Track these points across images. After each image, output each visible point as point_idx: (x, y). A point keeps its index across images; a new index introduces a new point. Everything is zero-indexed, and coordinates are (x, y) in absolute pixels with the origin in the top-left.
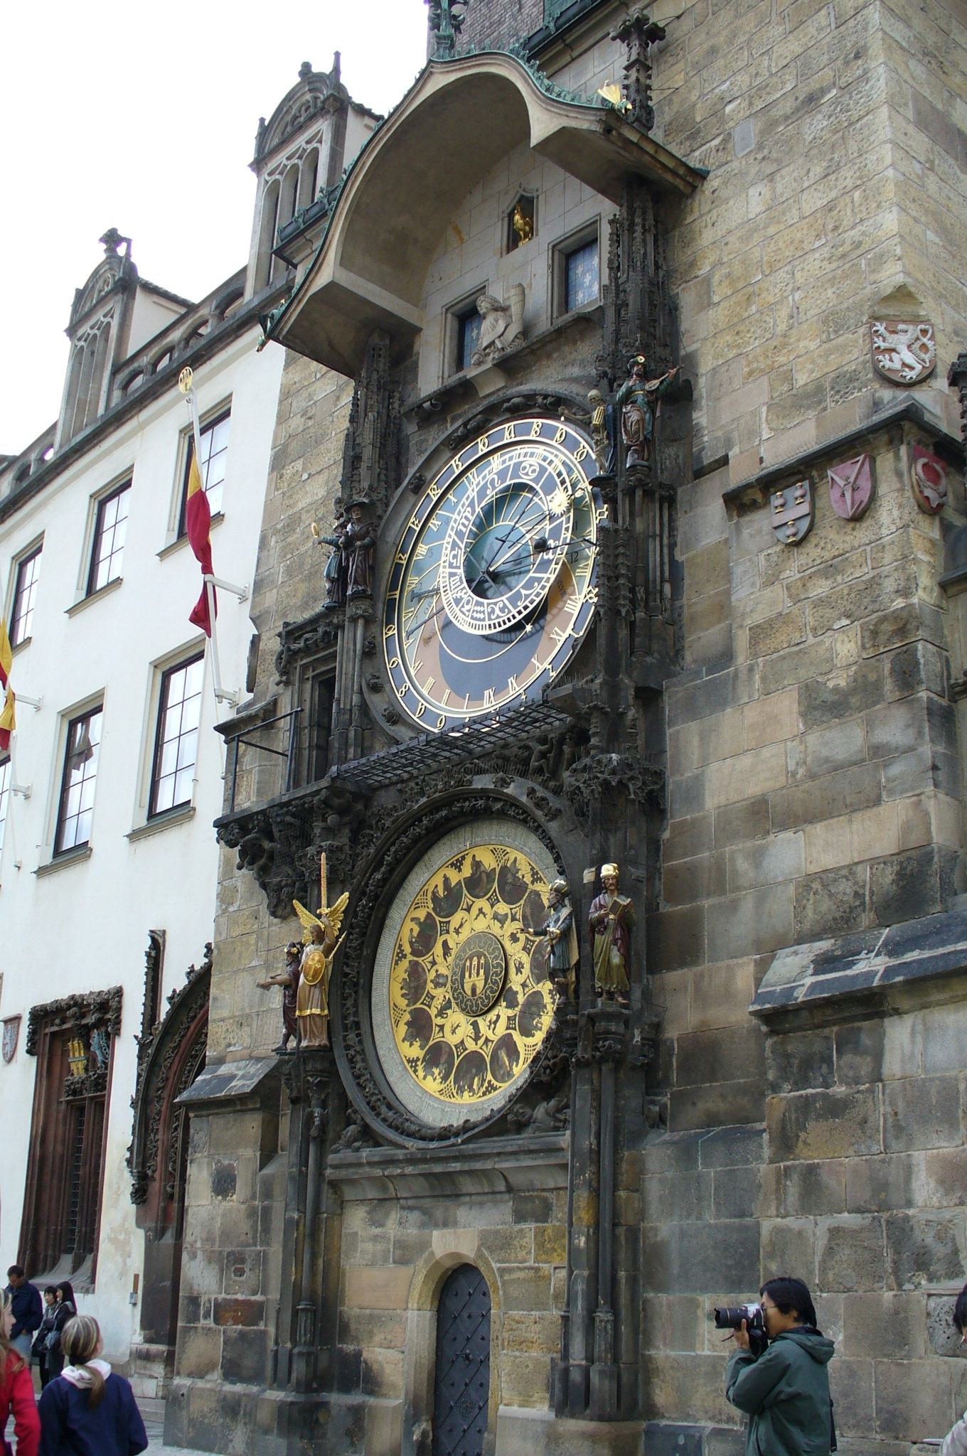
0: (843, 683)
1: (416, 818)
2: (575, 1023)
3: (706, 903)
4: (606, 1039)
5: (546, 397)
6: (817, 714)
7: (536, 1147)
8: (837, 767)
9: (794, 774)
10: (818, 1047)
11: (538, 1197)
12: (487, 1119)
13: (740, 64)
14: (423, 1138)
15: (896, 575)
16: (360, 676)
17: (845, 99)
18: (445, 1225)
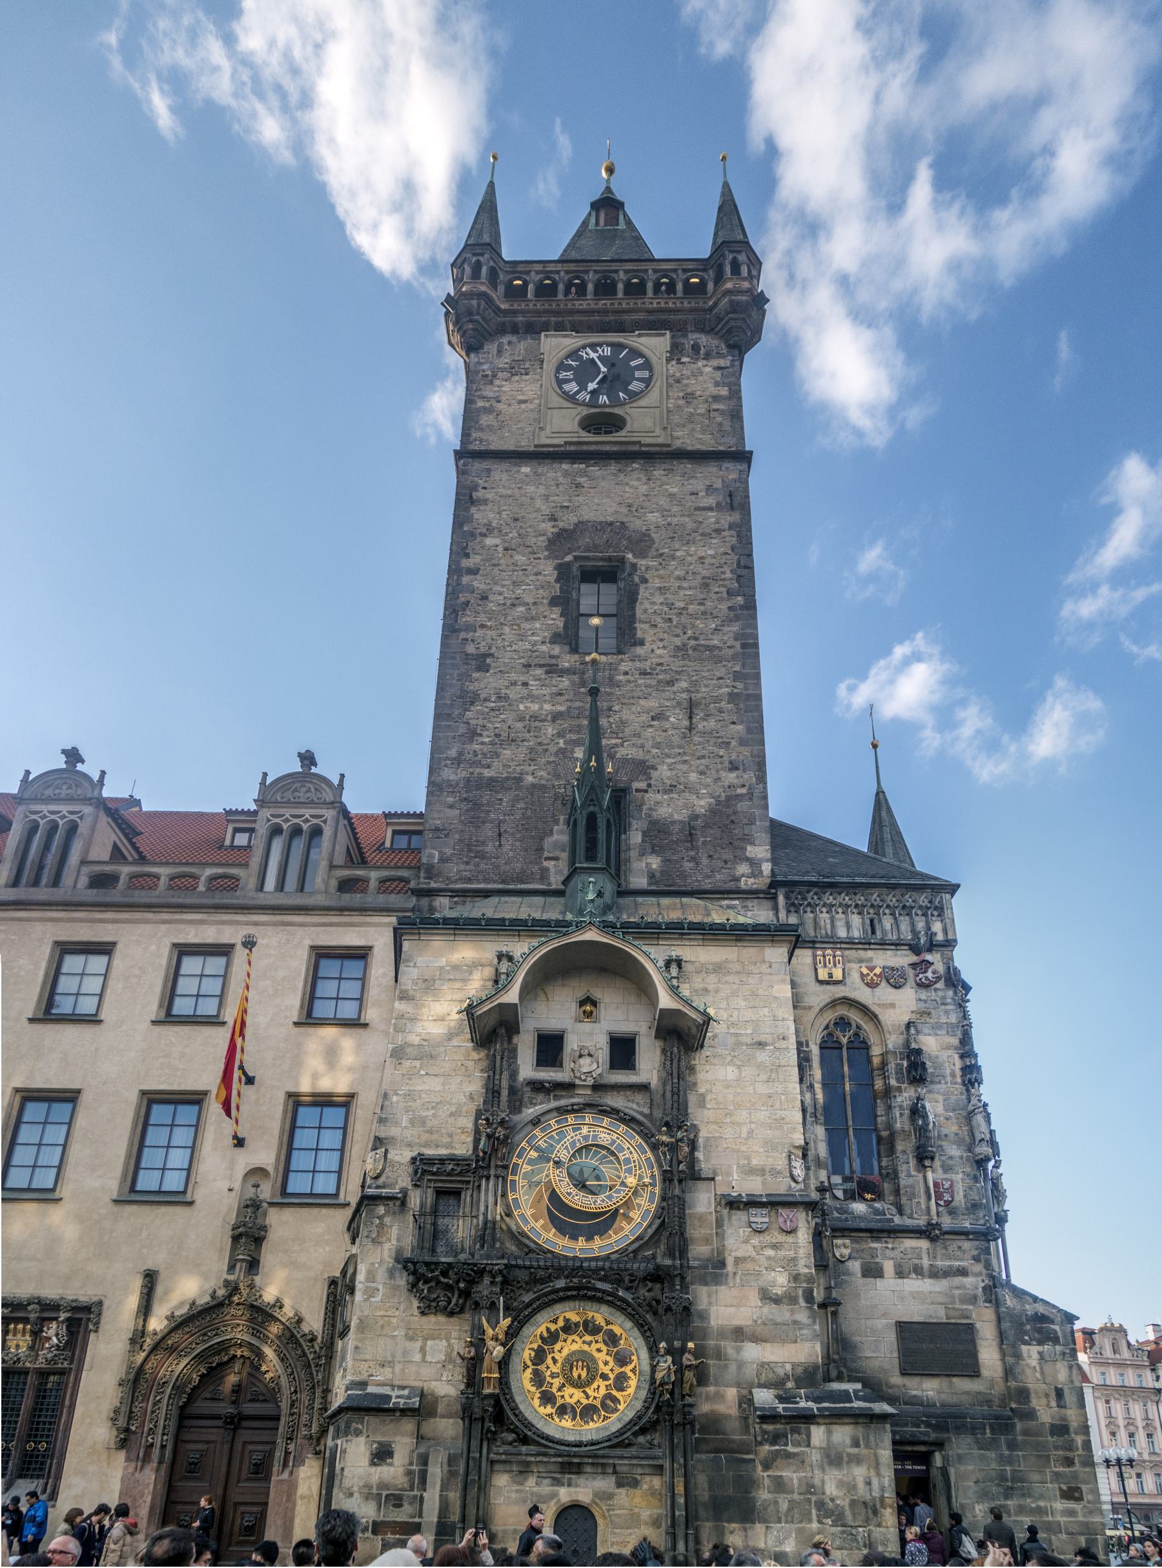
1: (557, 1291)
2: (673, 1406)
3: (711, 1362)
13: (721, 1006)
14: (562, 1444)
18: (569, 1485)
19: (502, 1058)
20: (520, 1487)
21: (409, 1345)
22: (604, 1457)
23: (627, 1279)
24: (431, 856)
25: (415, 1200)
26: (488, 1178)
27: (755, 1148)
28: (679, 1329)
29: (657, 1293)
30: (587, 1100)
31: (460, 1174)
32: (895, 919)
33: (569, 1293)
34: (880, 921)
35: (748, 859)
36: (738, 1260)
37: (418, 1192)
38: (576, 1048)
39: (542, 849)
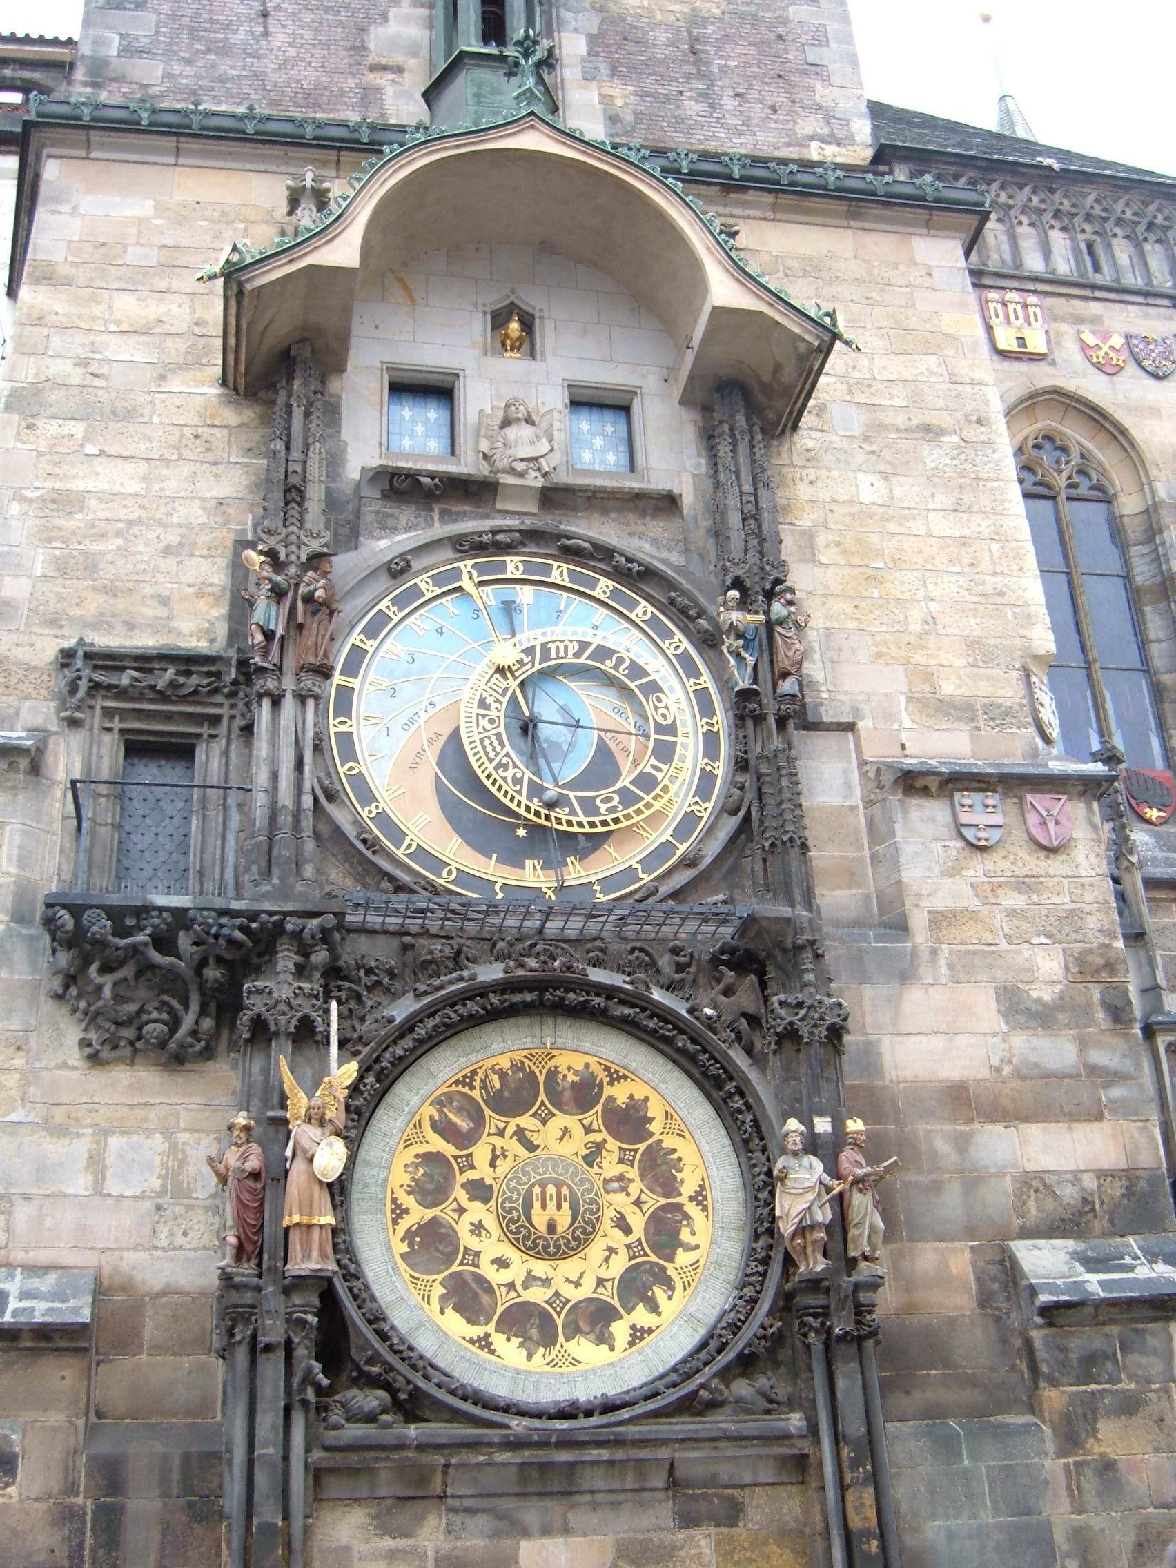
0: (1047, 998)
1: (483, 991)
2: (827, 1290)
4: (870, 1312)
5: (629, 560)
6: (1022, 1019)
7: (755, 1433)
8: (1048, 1075)
9: (998, 1070)
10: (1098, 1343)
11: (716, 1495)
12: (646, 1398)
14: (521, 1413)
15: (1099, 915)
16: (312, 772)
17: (970, 451)
18: (546, 1531)
19: (307, 415)
20: (402, 1543)
21: (54, 1148)
22: (643, 1443)
23: (665, 962)
24: (106, 43)
25: (67, 759)
26: (276, 702)
27: (946, 657)
28: (824, 1084)
29: (746, 998)
30: (529, 523)
31: (194, 696)
32: (1138, 244)
33: (517, 998)
34: (1109, 246)
35: (819, 108)
36: (938, 920)
37: (76, 739)
38: (488, 411)
39: (364, 48)
